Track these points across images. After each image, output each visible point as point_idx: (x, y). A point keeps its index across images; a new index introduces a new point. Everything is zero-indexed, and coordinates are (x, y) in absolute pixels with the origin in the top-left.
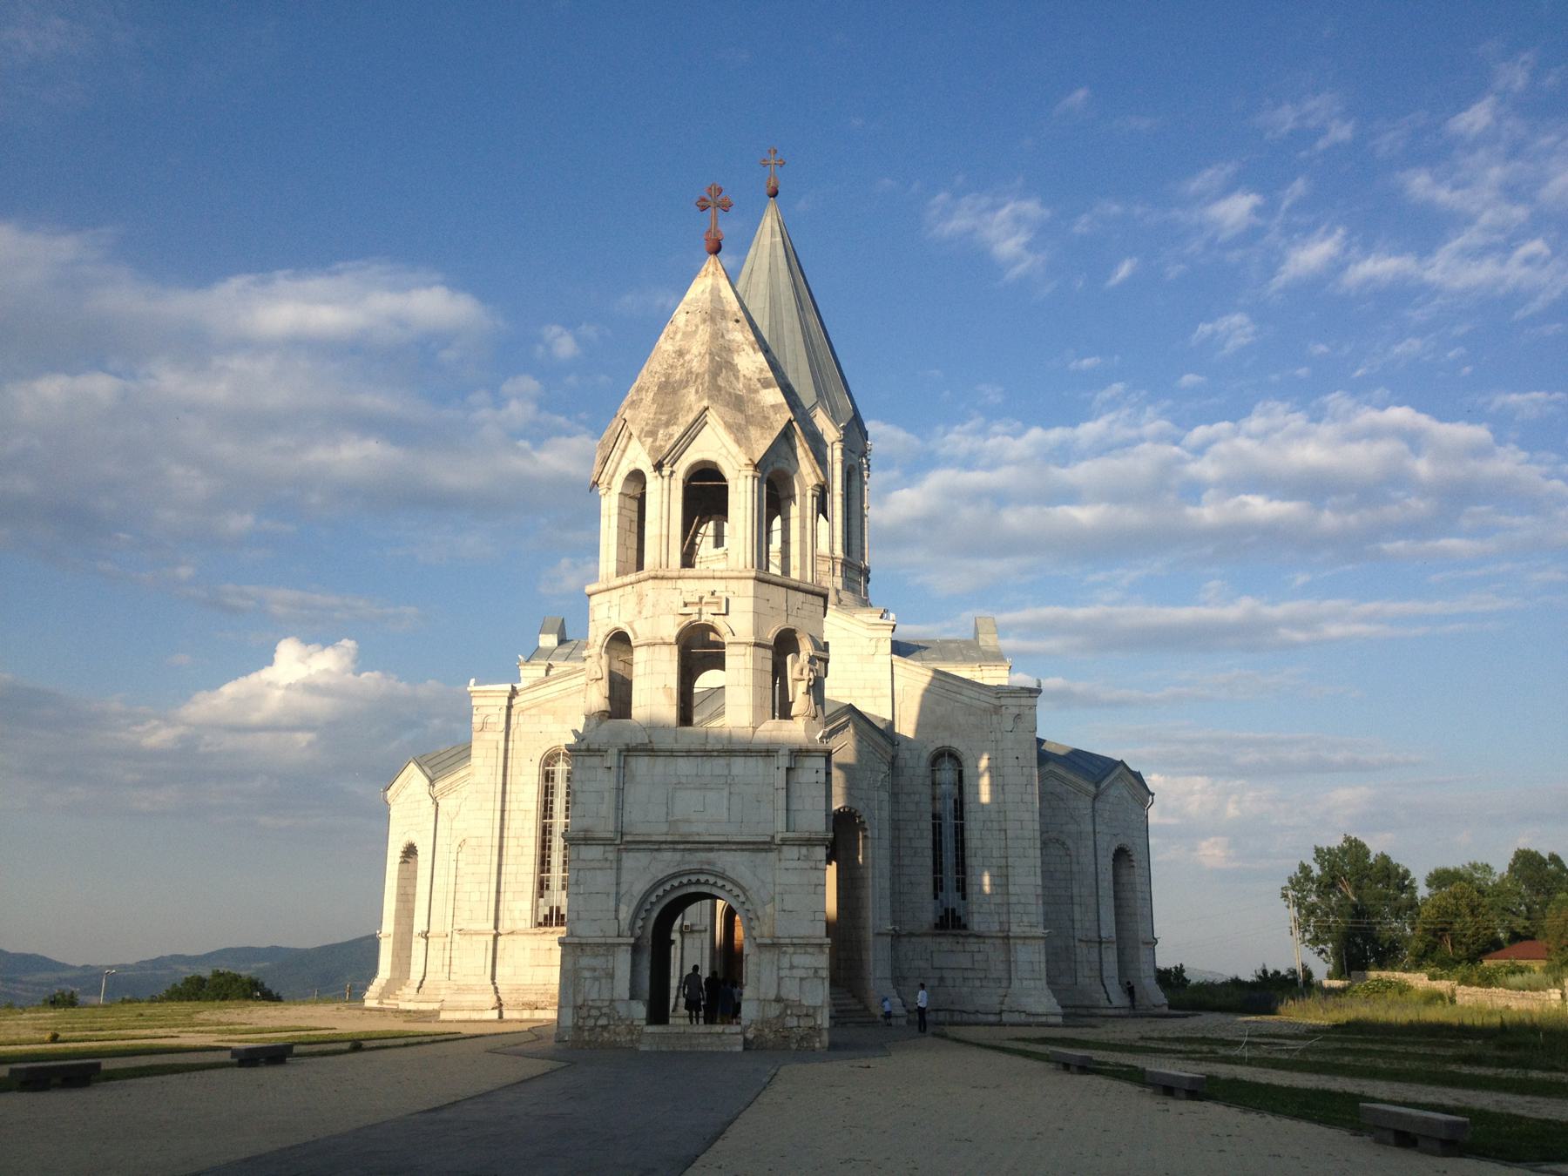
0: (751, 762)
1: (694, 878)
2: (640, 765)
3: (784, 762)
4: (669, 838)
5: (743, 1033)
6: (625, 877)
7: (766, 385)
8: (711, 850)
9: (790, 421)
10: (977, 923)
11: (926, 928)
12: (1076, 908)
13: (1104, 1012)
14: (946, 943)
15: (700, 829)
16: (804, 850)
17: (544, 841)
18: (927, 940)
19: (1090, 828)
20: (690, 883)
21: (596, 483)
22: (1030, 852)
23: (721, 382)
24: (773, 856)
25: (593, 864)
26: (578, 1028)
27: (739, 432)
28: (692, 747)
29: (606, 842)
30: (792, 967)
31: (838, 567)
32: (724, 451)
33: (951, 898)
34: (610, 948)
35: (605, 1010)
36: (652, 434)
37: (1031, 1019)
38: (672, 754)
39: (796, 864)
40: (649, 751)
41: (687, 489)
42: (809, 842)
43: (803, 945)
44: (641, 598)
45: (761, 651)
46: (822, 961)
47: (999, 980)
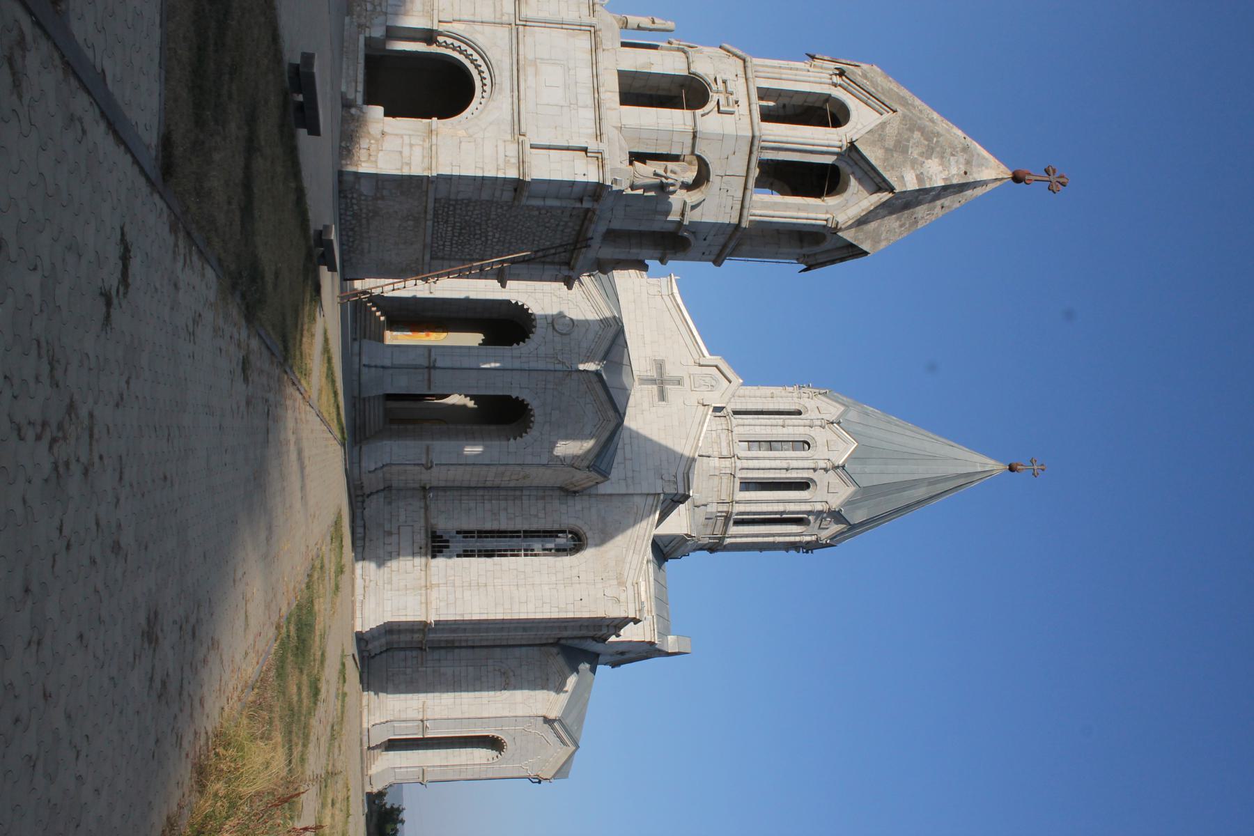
1: (488, 81)
2: (584, 42)
3: (592, 145)
4: (521, 57)
5: (356, 106)
6: (488, 29)
7: (920, 178)
9: (892, 190)
11: (433, 521)
13: (365, 719)
14: (421, 538)
15: (529, 80)
16: (514, 160)
18: (422, 523)
19: (520, 714)
20: (483, 79)
21: (813, 57)
22: (500, 610)
24: (509, 137)
27: (877, 133)
28: (600, 77)
30: (411, 145)
31: (725, 508)
32: (859, 126)
35: (378, 9)
37: (358, 605)
38: (595, 64)
39: (501, 155)
40: (595, 49)
42: (521, 162)
43: (431, 153)
46: (417, 170)
47: (390, 582)
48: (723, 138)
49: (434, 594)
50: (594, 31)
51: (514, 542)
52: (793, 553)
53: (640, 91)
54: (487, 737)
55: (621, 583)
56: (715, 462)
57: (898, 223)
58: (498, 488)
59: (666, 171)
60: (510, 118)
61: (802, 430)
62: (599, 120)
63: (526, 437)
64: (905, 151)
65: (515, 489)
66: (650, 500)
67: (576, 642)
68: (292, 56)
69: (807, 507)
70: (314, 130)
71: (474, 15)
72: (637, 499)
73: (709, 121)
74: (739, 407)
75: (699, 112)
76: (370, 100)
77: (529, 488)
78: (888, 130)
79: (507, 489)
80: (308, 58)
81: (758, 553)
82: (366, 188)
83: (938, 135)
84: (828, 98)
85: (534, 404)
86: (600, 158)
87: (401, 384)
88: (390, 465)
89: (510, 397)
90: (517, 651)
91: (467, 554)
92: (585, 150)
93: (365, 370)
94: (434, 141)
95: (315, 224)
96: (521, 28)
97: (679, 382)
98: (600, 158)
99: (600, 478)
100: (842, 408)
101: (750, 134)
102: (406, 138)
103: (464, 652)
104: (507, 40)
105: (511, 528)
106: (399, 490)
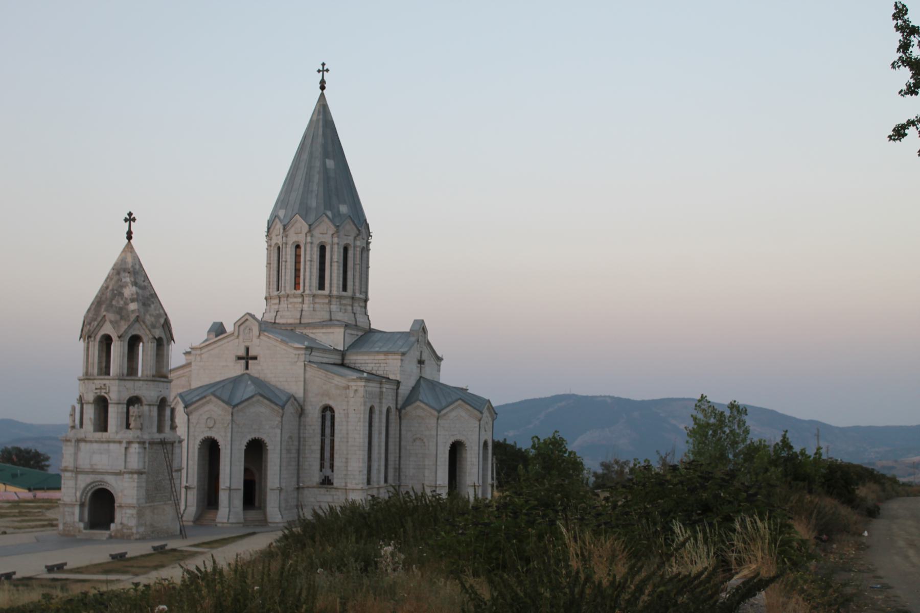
2: (82, 445)
3: (124, 445)
6: (79, 482)
7: (133, 301)
10: (337, 482)
11: (315, 484)
12: (427, 471)
14: (323, 491)
18: (315, 490)
19: (434, 433)
23: (114, 303)
26: (64, 530)
27: (115, 324)
29: (72, 471)
31: (334, 301)
33: (327, 472)
34: (73, 505)
38: (91, 442)
40: (84, 440)
45: (120, 406)
46: (134, 512)
48: (119, 392)
49: (350, 486)
50: (79, 441)
51: (328, 441)
52: (371, 246)
53: (102, 425)
54: (450, 451)
55: (348, 387)
56: (305, 307)
57: (153, 306)
58: (298, 451)
61: (289, 249)
62: (114, 442)
63: (267, 440)
64: (121, 309)
65: (299, 442)
66: (308, 369)
67: (400, 399)
68: (110, 559)
69: (336, 248)
70: (126, 553)
72: (308, 376)
73: (113, 396)
74: (275, 286)
76: (108, 528)
77: (299, 433)
78: (113, 319)
79: (299, 445)
80: (111, 555)
81: (370, 270)
82: (142, 530)
83: (113, 290)
84: (101, 342)
85: (249, 437)
86: (129, 443)
87: (239, 501)
88: (280, 507)
89: (246, 451)
90: (403, 432)
91: (332, 466)
92: (126, 448)
93: (230, 521)
95: (152, 551)
97: (248, 349)
98: (129, 443)
99: (292, 399)
100: (277, 220)
103: (402, 462)
105: (320, 444)
106: (298, 500)
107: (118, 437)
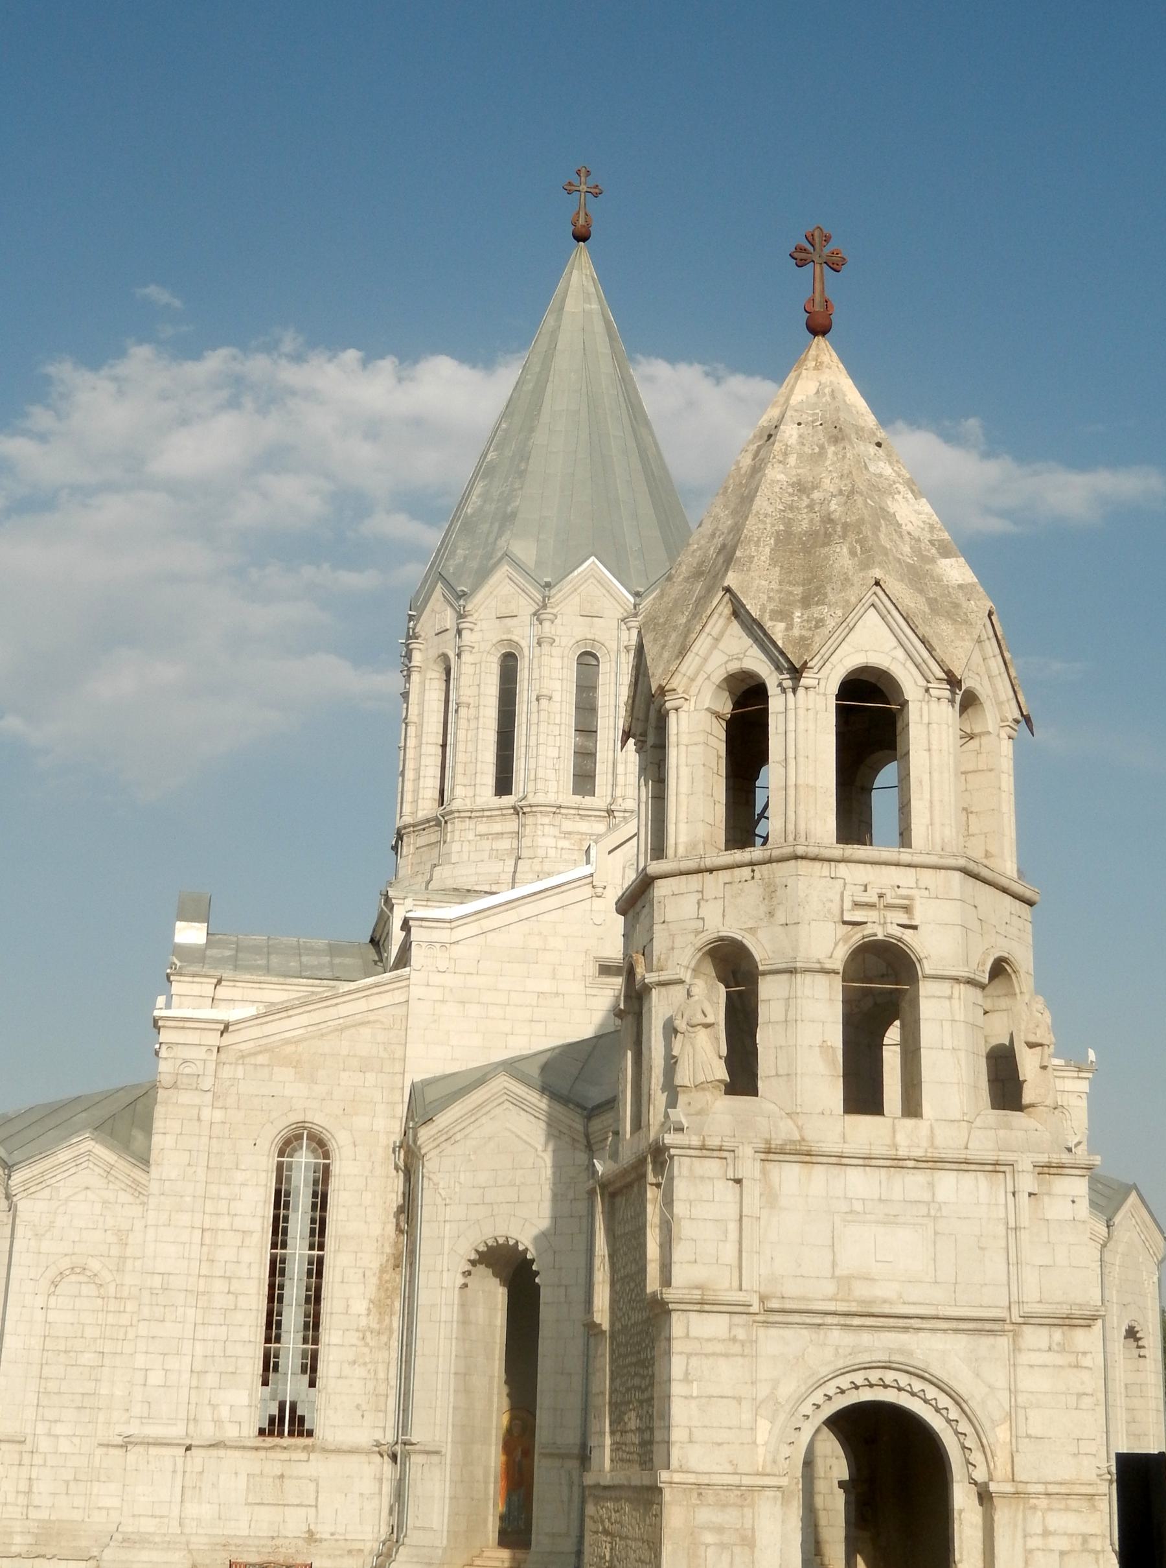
0: (968, 1179)
2: (789, 1175)
3: (1027, 1183)
4: (842, 1307)
8: (906, 1329)
15: (886, 1293)
16: (1057, 1334)
17: (272, 1287)
24: (1003, 1342)
25: (709, 1348)
28: (878, 1151)
30: (1046, 1533)
36: (782, 615)
38: (840, 1160)
40: (804, 1154)
41: (843, 714)
42: (1069, 1322)
43: (1062, 1495)
44: (771, 891)
59: (1031, 1045)
60: (963, 1338)
62: (964, 1164)
71: (739, 1400)
75: (927, 967)
94: (1040, 1488)
96: (774, 1304)
101: (957, 875)
102: (1034, 1543)
104: (788, 1333)
107: (983, 1146)
